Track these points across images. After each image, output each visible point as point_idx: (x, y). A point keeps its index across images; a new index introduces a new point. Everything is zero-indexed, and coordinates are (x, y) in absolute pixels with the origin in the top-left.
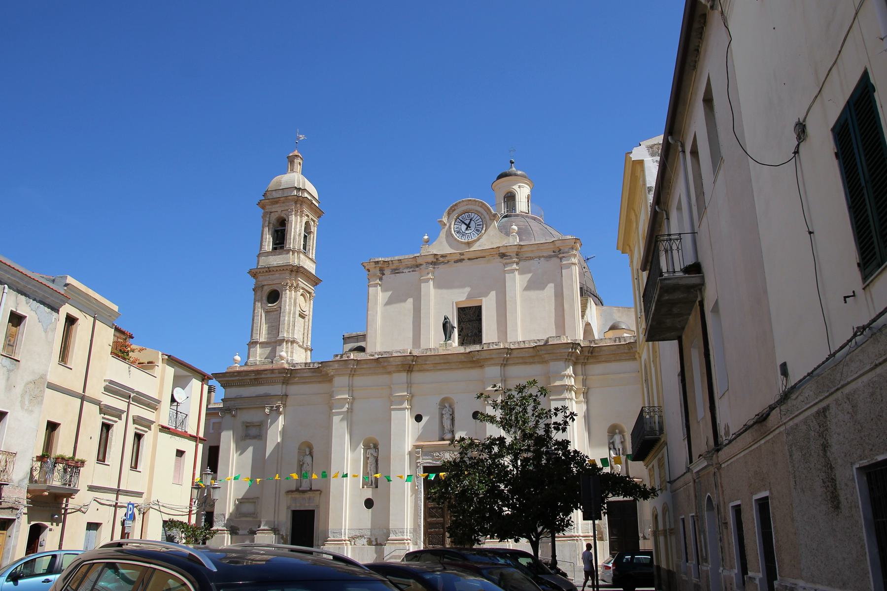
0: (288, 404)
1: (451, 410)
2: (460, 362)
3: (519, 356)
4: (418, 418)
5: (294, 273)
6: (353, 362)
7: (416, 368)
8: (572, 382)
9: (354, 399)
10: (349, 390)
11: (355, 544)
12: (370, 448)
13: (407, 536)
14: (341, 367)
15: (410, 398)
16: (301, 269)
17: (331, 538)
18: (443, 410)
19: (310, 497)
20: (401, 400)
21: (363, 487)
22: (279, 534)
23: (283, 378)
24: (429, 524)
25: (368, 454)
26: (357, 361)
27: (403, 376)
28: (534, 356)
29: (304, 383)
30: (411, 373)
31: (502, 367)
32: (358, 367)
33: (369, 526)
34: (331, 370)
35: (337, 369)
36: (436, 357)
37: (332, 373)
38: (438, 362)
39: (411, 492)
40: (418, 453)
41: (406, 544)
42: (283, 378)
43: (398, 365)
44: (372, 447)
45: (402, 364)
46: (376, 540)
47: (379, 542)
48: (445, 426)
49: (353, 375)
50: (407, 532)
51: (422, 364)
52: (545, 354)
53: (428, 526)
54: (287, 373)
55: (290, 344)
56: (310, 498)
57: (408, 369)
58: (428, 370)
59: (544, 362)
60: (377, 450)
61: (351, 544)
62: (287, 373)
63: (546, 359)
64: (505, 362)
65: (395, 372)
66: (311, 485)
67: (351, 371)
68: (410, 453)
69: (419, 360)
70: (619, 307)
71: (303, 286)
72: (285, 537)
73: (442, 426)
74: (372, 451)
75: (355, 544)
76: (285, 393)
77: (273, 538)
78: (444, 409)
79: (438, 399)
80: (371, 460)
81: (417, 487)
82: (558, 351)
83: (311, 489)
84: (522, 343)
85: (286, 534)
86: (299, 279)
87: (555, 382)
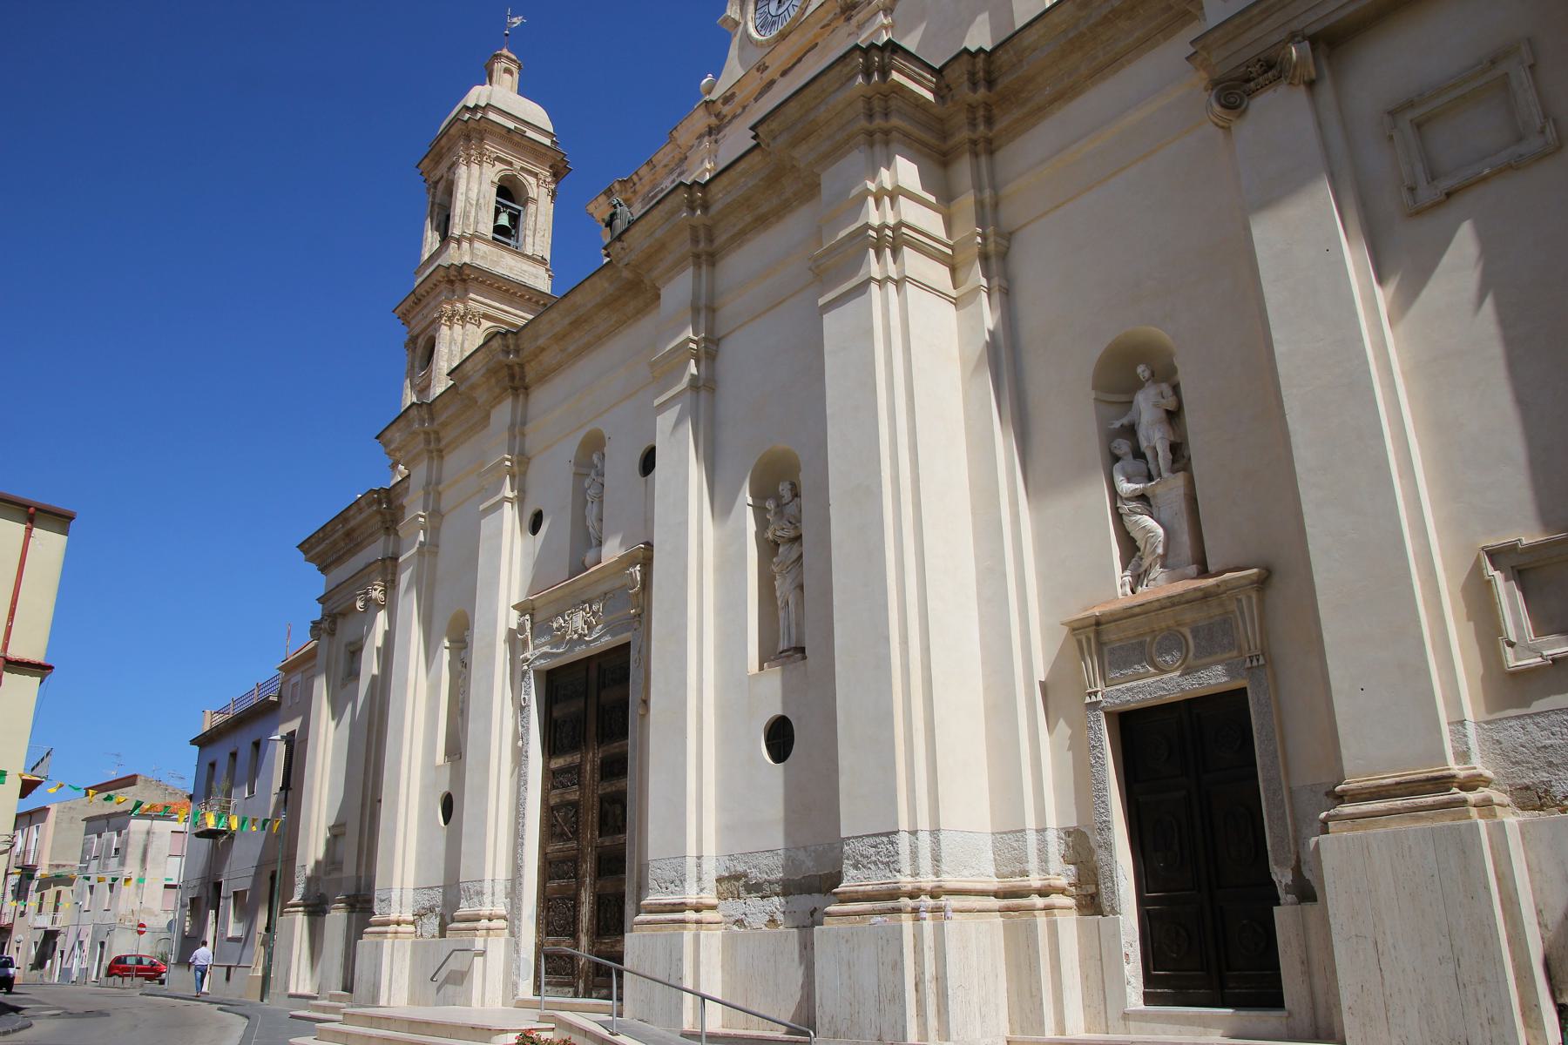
5: (458, 286)
7: (530, 375)
16: (467, 272)
49: (440, 451)
58: (556, 369)
62: (380, 502)
67: (428, 442)
71: (483, 309)
76: (392, 554)
86: (472, 295)
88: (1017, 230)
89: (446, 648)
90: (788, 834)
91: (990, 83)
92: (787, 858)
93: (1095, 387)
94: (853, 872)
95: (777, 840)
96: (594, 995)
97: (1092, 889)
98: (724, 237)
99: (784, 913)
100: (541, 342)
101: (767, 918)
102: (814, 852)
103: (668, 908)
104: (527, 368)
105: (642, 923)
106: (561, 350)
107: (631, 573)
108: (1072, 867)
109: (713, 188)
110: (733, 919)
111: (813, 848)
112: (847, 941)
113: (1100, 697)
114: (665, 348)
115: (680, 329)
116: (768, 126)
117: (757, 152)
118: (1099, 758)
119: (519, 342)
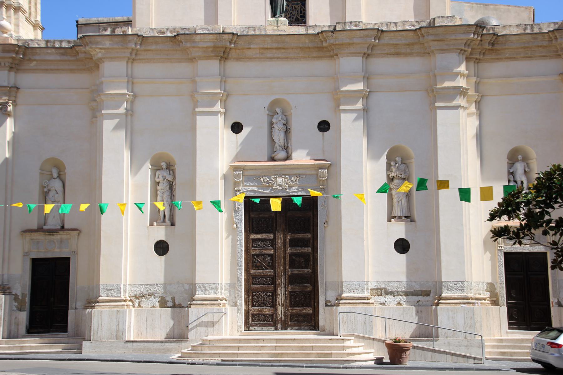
0: (19, 101)
1: (285, 119)
2: (301, 48)
3: (391, 42)
4: (237, 128)
6: (135, 38)
7: (233, 54)
8: (462, 82)
9: (135, 96)
10: (128, 82)
11: (140, 306)
12: (160, 169)
13: (222, 293)
14: (115, 46)
15: (224, 98)
17: (103, 296)
18: (273, 118)
19: (61, 239)
20: (211, 100)
21: (151, 224)
22: (10, 293)
23: (11, 60)
24: (253, 278)
25: (158, 177)
26: (141, 38)
27: (214, 66)
28: (413, 44)
29: (46, 71)
30: (224, 61)
31: (365, 59)
32: (143, 48)
34: (98, 50)
35: (108, 49)
36: (267, 39)
37: (100, 55)
38: (269, 46)
40: (238, 176)
42: (11, 60)
43: (207, 47)
44: (164, 167)
45: (215, 47)
46: (173, 299)
47: (177, 303)
48: (276, 141)
49: (134, 60)
51: (243, 49)
52: (433, 41)
53: (251, 280)
54: (17, 53)
55: (12, 11)
56: (61, 241)
57: (222, 55)
58: (251, 59)
59: (426, 53)
60: (171, 172)
61: (134, 306)
62: (17, 53)
63: (432, 49)
64: (369, 52)
65: (200, 58)
66: (63, 222)
67: (131, 54)
68: (225, 177)
69: (241, 42)
70: (472, 4)
72: (20, 297)
74: (166, 173)
75: (140, 306)
77: (1, 299)
78: (275, 117)
79: (266, 101)
80: (163, 187)
81: (235, 226)
82: (453, 37)
83: (63, 227)
84: (393, 25)
85: (23, 294)
87: (443, 82)
88: (485, 96)
89: (150, 168)
90: (407, 277)
91: (493, 45)
92: (407, 285)
93: (508, 158)
94: (446, 291)
95: (403, 279)
97: (495, 299)
98: (379, 52)
99: (405, 301)
100: (252, 46)
101: (397, 303)
102: (419, 283)
103: (357, 298)
104: (233, 52)
105: (343, 303)
106: (260, 53)
107: (323, 172)
108: (489, 293)
109: (385, 34)
111: (419, 282)
112: (452, 311)
113: (503, 248)
114: (346, 86)
115: (358, 81)
116: (428, 30)
117: (413, 32)
118: (501, 264)
119: (237, 40)
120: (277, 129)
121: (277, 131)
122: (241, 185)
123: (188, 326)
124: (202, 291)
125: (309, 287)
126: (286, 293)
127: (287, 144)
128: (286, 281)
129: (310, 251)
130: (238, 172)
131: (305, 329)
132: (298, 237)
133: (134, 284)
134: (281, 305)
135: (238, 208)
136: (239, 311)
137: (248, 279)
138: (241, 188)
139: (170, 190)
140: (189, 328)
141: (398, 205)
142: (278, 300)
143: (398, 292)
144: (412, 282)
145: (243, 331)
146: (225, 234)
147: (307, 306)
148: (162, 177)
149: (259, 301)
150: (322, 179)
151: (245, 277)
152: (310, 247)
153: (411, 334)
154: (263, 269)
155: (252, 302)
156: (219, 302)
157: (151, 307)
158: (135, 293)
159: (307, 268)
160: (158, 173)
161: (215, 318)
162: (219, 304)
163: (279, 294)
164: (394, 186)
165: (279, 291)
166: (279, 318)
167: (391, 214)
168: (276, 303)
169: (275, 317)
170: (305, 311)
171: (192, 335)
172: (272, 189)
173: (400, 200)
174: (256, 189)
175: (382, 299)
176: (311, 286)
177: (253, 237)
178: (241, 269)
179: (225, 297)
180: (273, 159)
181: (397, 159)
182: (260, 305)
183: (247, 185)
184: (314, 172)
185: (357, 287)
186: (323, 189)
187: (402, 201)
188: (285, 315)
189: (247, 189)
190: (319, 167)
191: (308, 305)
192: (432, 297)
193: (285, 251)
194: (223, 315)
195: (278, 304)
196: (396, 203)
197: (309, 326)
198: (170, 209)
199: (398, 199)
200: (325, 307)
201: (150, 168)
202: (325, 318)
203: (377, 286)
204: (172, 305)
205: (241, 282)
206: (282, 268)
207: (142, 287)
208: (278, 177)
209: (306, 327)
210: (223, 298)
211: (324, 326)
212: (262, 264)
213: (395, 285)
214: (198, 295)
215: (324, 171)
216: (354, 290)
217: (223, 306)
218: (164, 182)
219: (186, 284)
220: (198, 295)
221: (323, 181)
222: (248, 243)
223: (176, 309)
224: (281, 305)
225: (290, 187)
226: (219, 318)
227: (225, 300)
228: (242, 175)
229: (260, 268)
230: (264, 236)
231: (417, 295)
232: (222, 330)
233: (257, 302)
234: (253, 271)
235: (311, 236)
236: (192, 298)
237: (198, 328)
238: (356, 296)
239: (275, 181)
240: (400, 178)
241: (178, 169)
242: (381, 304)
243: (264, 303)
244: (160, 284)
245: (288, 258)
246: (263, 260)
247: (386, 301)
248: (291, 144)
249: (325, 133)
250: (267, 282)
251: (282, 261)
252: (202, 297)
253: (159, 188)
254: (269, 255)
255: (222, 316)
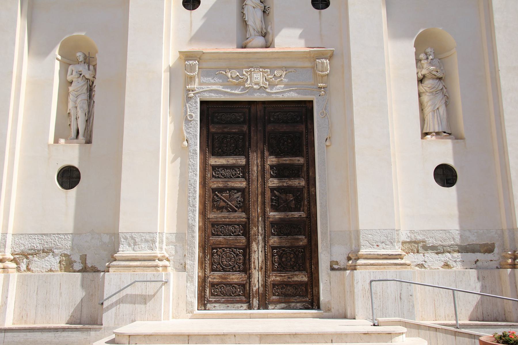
11: (28, 269)
13: (161, 249)
21: (56, 141)
24: (213, 225)
33: (69, 226)
39: (173, 153)
40: (191, 68)
41: (160, 269)
44: (81, 59)
46: (84, 259)
50: (161, 242)
60: (91, 67)
61: (18, 269)
68: (172, 71)
73: (244, 23)
74: (83, 68)
75: (28, 269)
81: (185, 143)
89: (57, 59)
96: (270, 307)
101: (443, 264)
102: (476, 232)
103: (384, 257)
105: (362, 265)
107: (323, 63)
110: (415, 264)
111: (475, 231)
120: (251, 6)
121: (251, 9)
122: (197, 80)
123: (102, 304)
124: (129, 245)
125: (303, 241)
126: (265, 249)
127: (266, 29)
128: (265, 230)
129: (303, 183)
130: (191, 62)
131: (297, 307)
132: (284, 162)
133: (22, 234)
134: (257, 268)
135: (191, 116)
136: (190, 278)
137: (205, 228)
138: (195, 86)
139: (87, 92)
140: (104, 307)
141: (433, 116)
142: (253, 260)
143: (443, 246)
144: (464, 231)
145: (196, 312)
146: (169, 155)
147: (299, 270)
148: (77, 72)
149: (222, 262)
150: (321, 73)
151: (201, 224)
152: (302, 177)
153: (469, 314)
154: (229, 211)
155: (212, 264)
156: (157, 262)
157: (46, 272)
158: (23, 248)
159: (299, 210)
160: (70, 68)
161: (151, 289)
162: (157, 266)
163: (255, 252)
164: (426, 88)
165: (254, 246)
166: (255, 289)
167: (422, 131)
168: (250, 265)
169: (248, 288)
170: (296, 279)
171: (108, 318)
172: (245, 89)
173: (436, 108)
174: (220, 88)
175: (419, 258)
176: (306, 238)
177: (214, 161)
178: (194, 211)
179: (167, 255)
180: (245, 47)
181: (429, 50)
182: (223, 268)
183: (205, 83)
184: (308, 64)
185: (383, 239)
186: (323, 88)
187: (440, 109)
188: (265, 286)
189: (205, 88)
190: (317, 57)
191: (301, 268)
192: (498, 254)
193: (264, 183)
194: (162, 285)
195: (253, 266)
196: (431, 114)
197: (303, 302)
198: (87, 121)
199: (434, 108)
200: (329, 271)
201: (57, 59)
202: (330, 289)
203: (411, 237)
204: (81, 268)
205: (193, 232)
206: (259, 211)
207: (35, 239)
208: (253, 70)
209: (298, 305)
210: (162, 256)
211: (329, 302)
212: (228, 204)
213: (439, 235)
214: (123, 251)
215: (325, 61)
216: (379, 244)
217: (163, 270)
218: (80, 79)
219: (105, 233)
220: (123, 251)
221: (322, 76)
222: (206, 172)
223: (86, 274)
224: (257, 268)
225: (272, 85)
226: (156, 290)
227: (168, 260)
228: (197, 67)
229: (224, 210)
230: (230, 160)
231: (473, 251)
232: (161, 310)
233: (219, 264)
234: (212, 215)
235: (304, 161)
236: (112, 257)
237: (118, 306)
238: (383, 253)
239: (249, 76)
240: (434, 77)
241: (100, 61)
242: (418, 265)
243: (230, 265)
244: (63, 234)
245: (268, 194)
246: (230, 198)
247: (425, 262)
248: (272, 27)
249: (323, 11)
250: (235, 232)
251: (259, 199)
252: (128, 255)
253: (71, 89)
254: (238, 190)
255: (161, 287)
